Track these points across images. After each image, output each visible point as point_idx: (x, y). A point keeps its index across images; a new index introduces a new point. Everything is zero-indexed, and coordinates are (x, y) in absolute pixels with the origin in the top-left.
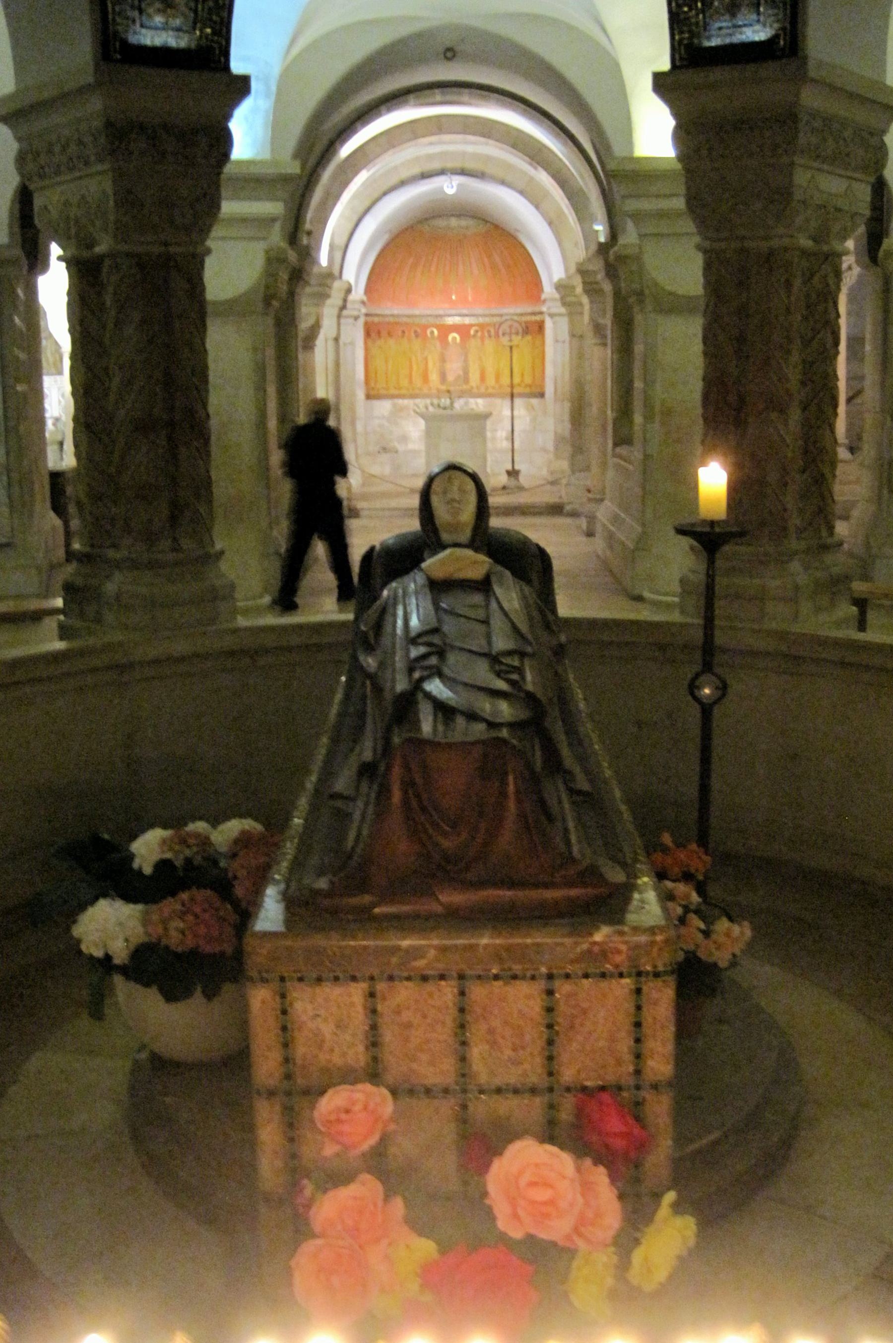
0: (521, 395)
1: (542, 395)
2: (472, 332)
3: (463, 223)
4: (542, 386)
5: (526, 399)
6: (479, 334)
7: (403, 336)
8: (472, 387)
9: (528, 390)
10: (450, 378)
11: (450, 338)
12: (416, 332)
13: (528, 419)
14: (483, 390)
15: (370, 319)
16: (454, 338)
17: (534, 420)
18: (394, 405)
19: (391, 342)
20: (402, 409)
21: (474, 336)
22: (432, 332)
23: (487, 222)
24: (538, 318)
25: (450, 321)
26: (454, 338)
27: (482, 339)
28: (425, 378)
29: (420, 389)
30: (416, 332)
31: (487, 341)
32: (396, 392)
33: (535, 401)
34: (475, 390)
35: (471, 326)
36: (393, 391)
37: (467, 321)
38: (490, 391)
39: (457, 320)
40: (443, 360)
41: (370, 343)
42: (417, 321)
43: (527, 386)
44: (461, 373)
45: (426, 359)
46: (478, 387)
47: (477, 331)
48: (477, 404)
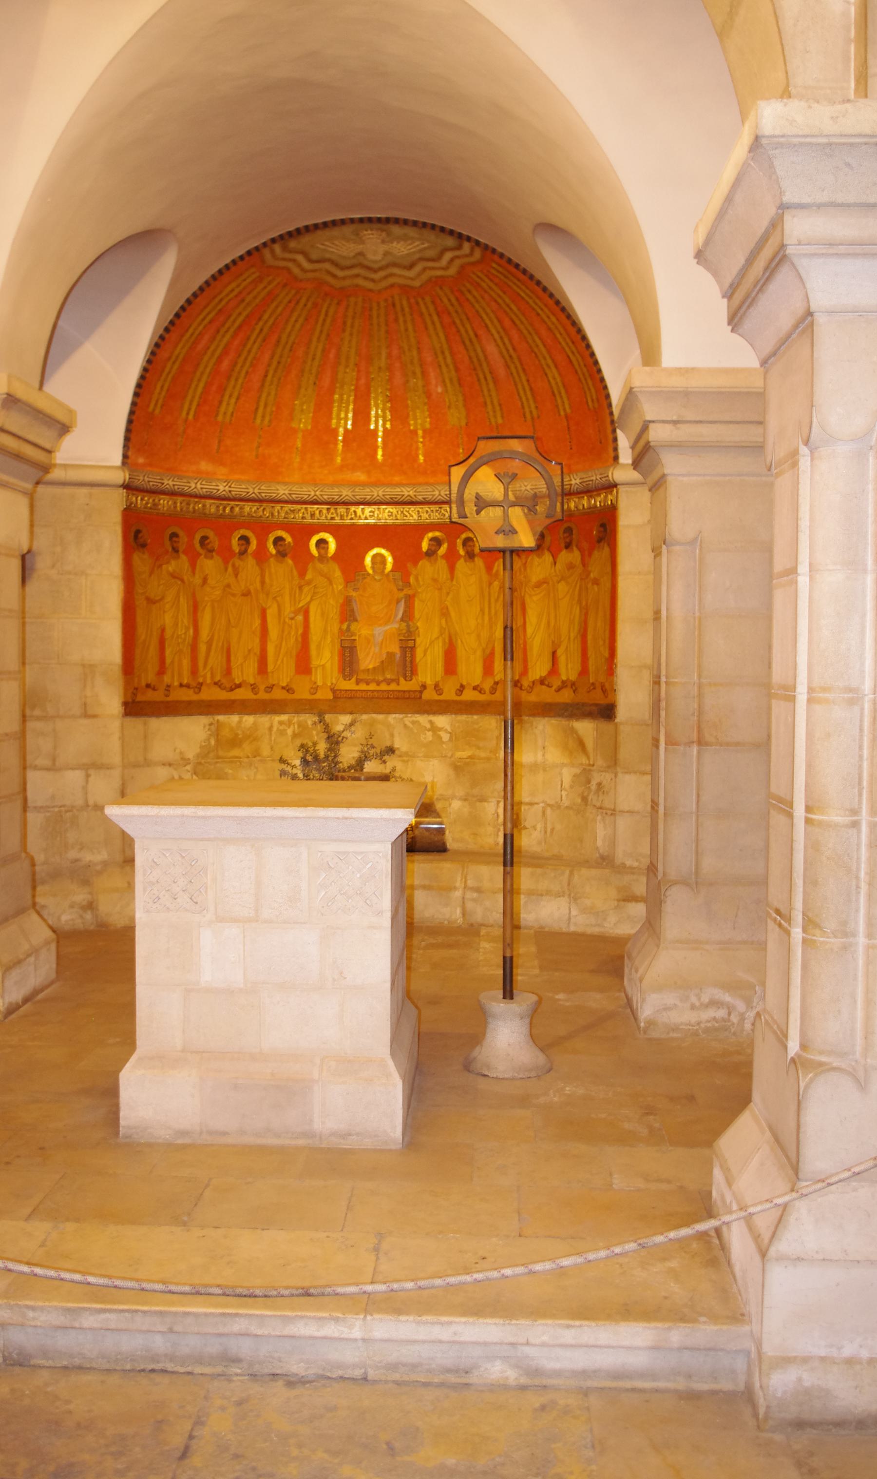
0: (547, 710)
1: (607, 712)
2: (425, 546)
3: (401, 249)
4: (607, 689)
5: (564, 722)
6: (443, 550)
7: (243, 553)
8: (424, 687)
9: (566, 696)
10: (367, 660)
11: (368, 560)
12: (278, 540)
13: (567, 775)
14: (449, 694)
15: (139, 501)
16: (379, 560)
17: (584, 777)
18: (217, 731)
19: (210, 565)
20: (235, 742)
21: (431, 554)
22: (322, 543)
23: (460, 236)
24: (598, 501)
25: (367, 516)
26: (379, 560)
27: (451, 558)
28: (303, 665)
29: (288, 689)
30: (278, 540)
31: (461, 565)
32: (223, 695)
33: (585, 728)
34: (429, 695)
35: (421, 529)
36: (210, 694)
37: (412, 515)
38: (469, 695)
39: (385, 515)
40: (348, 613)
41: (141, 561)
42: (280, 512)
43: (564, 685)
44: (395, 649)
45: (306, 613)
46: (437, 687)
47: (437, 542)
48: (434, 729)
